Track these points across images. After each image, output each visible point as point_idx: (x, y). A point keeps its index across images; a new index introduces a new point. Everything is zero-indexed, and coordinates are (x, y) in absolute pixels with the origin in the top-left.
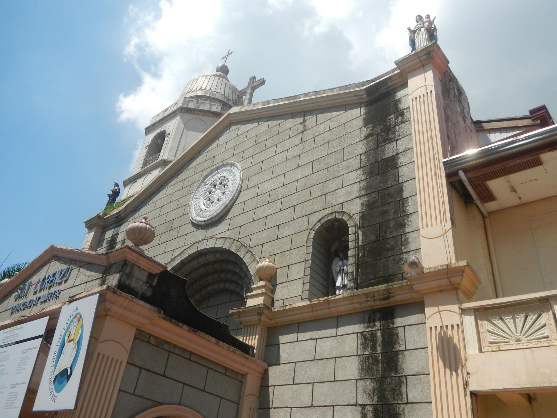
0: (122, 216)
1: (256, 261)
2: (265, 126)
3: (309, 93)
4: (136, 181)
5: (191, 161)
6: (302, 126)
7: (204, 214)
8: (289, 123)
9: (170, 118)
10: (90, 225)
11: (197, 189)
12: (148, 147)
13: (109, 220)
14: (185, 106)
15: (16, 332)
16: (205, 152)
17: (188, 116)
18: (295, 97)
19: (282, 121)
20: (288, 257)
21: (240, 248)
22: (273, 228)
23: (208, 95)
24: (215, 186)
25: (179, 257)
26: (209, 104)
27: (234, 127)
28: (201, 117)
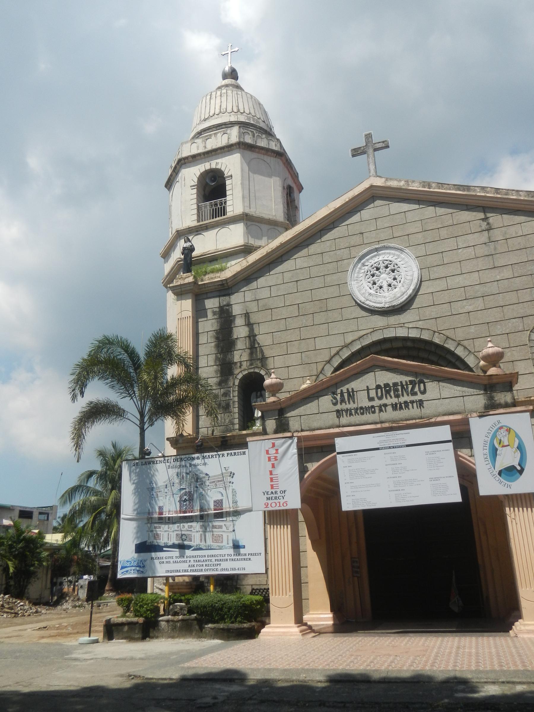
0: (229, 284)
1: (472, 355)
2: (430, 211)
3: (487, 187)
4: (199, 233)
5: (322, 232)
6: (486, 223)
7: (374, 298)
8: (466, 216)
9: (222, 153)
10: (181, 291)
11: (353, 269)
12: (196, 187)
13: (208, 287)
14: (242, 140)
15: (398, 437)
16: (343, 224)
17: (248, 153)
18: (468, 188)
19: (455, 211)
20: (509, 354)
21: (446, 340)
22: (481, 325)
23: (252, 122)
24: (378, 269)
25: (358, 342)
26: (266, 139)
27: (378, 202)
28: (262, 156)
